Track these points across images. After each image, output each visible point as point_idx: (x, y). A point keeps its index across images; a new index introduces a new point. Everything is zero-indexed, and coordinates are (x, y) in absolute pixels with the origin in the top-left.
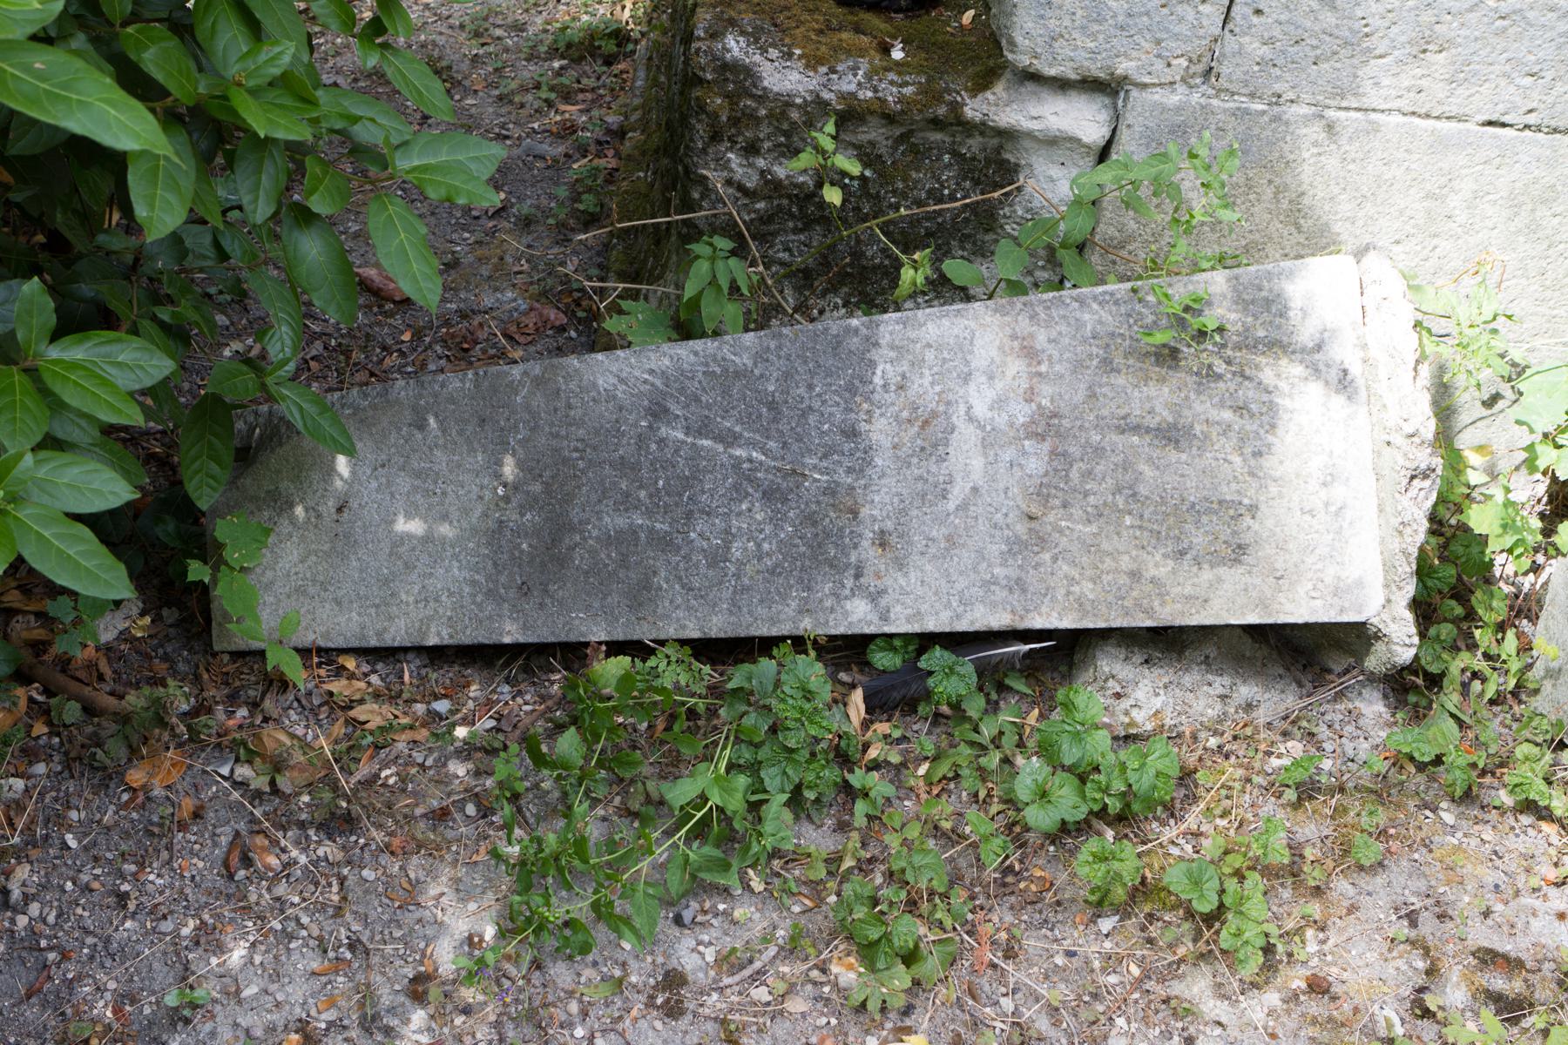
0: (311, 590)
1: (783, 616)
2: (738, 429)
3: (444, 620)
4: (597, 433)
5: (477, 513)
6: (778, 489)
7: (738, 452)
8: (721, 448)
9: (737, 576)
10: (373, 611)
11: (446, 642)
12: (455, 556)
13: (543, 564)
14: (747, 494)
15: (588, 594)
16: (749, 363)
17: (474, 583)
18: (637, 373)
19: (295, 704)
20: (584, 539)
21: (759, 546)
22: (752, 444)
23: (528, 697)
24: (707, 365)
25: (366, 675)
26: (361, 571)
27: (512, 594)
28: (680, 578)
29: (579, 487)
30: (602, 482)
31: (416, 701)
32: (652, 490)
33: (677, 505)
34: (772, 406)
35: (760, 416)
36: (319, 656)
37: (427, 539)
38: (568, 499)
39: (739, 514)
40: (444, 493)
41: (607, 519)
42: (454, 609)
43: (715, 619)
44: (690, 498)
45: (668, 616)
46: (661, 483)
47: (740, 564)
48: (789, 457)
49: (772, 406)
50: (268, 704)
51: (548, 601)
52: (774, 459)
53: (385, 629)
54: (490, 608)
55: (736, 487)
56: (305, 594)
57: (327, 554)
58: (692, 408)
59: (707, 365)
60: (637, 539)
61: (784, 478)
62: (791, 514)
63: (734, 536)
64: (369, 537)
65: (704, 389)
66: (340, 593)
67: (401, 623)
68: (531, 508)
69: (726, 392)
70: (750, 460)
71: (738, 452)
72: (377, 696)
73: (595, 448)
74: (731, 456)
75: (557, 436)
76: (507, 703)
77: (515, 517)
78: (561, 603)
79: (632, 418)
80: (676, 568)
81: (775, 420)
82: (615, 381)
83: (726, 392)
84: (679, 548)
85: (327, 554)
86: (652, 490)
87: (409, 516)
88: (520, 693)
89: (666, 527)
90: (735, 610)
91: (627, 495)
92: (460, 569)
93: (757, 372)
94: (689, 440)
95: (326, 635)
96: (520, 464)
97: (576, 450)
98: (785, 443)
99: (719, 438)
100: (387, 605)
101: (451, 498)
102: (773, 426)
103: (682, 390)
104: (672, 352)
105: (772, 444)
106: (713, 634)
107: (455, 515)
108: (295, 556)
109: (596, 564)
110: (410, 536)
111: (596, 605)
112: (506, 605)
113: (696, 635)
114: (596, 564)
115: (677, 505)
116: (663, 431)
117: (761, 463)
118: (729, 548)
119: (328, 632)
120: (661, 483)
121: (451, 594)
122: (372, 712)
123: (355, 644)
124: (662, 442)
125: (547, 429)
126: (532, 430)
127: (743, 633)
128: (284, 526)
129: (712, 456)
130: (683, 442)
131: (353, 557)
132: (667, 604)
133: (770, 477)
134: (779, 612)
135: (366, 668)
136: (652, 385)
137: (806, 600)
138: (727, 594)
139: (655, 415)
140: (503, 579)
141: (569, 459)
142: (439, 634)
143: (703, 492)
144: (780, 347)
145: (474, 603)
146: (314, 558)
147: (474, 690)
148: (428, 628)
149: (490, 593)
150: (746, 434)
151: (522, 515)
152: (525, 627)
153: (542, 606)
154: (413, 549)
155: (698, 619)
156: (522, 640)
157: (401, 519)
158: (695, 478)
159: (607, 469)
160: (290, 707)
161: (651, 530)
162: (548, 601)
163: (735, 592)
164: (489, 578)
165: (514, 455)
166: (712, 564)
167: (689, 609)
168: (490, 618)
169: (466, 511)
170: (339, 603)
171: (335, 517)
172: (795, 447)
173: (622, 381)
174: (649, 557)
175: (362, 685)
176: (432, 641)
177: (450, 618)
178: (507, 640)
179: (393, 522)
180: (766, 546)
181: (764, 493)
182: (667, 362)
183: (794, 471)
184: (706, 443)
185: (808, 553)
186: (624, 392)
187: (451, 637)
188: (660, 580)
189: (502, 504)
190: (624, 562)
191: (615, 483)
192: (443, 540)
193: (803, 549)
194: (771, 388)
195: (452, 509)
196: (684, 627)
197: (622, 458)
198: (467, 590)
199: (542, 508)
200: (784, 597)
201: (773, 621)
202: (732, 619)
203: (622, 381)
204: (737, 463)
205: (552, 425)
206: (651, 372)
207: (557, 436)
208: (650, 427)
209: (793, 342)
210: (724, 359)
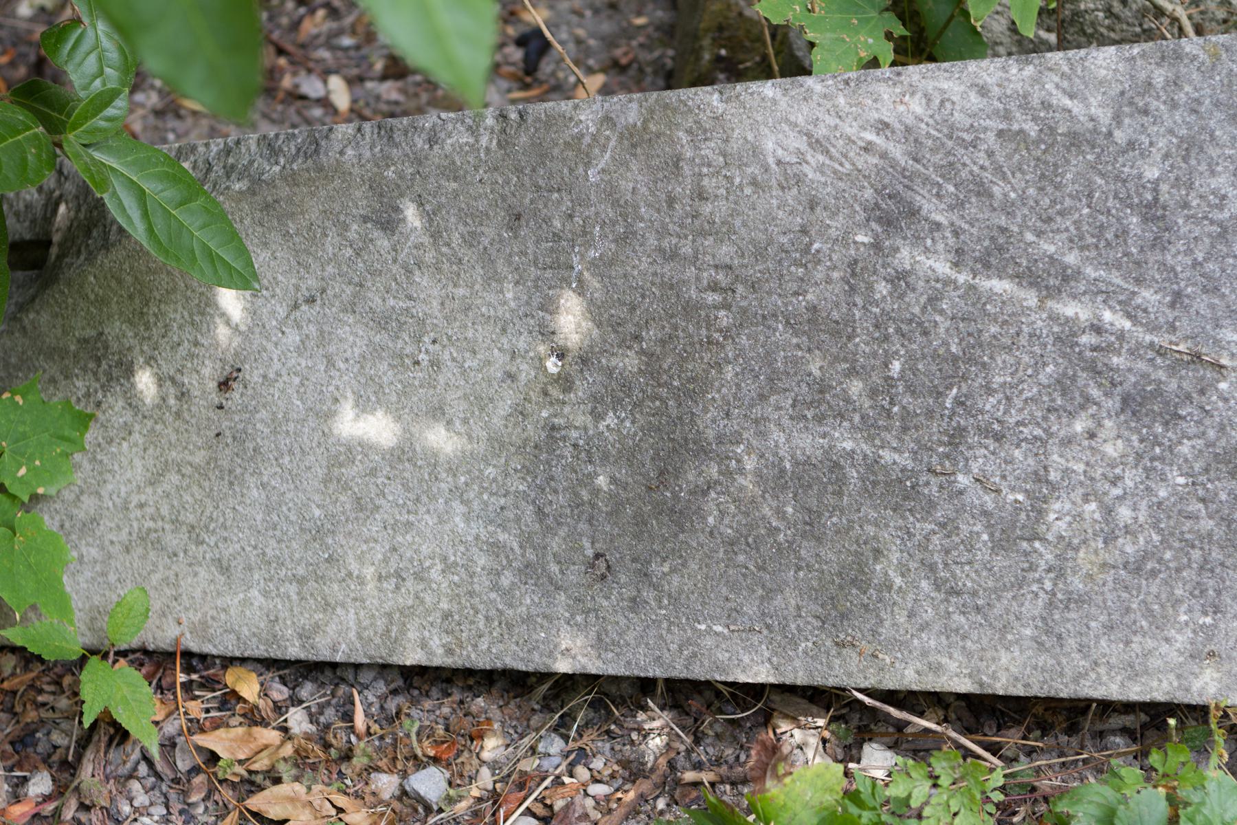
0: (172, 541)
1: (1153, 663)
2: (1071, 259)
3: (436, 617)
4: (760, 254)
5: (504, 408)
6: (1158, 392)
7: (1070, 309)
8: (1031, 298)
9: (1058, 572)
10: (292, 589)
11: (437, 662)
12: (458, 493)
13: (640, 521)
14: (1088, 400)
15: (734, 586)
16: (1104, 117)
17: (495, 548)
18: (850, 129)
19: (143, 769)
20: (728, 473)
21: (1108, 511)
22: (1107, 295)
23: (598, 764)
24: (1007, 116)
25: (278, 708)
26: (268, 509)
27: (575, 574)
28: (932, 568)
29: (719, 366)
30: (768, 358)
31: (377, 769)
32: (876, 379)
33: (930, 414)
34: (1153, 212)
35: (1123, 234)
36: (188, 669)
37: (402, 454)
38: (695, 389)
39: (1068, 442)
40: (435, 364)
41: (777, 436)
42: (455, 598)
43: (1004, 658)
44: (959, 402)
45: (903, 645)
46: (896, 366)
47: (1066, 546)
48: (1184, 326)
49: (1153, 212)
50: (87, 772)
51: (649, 595)
52: (1153, 328)
53: (317, 627)
54: (528, 600)
55: (1063, 384)
56: (158, 545)
57: (201, 472)
58: (972, 210)
59: (1007, 116)
60: (842, 481)
61: (1172, 370)
62: (1185, 449)
63: (1054, 487)
64: (284, 442)
65: (998, 170)
66: (228, 551)
67: (349, 617)
68: (617, 403)
69: (1048, 178)
70: (1097, 329)
71: (1070, 309)
72: (301, 761)
73: (753, 287)
74: (1054, 318)
75: (673, 256)
76: (558, 782)
77: (580, 420)
78: (675, 600)
79: (836, 225)
80: (923, 547)
81: (1158, 244)
82: (802, 144)
83: (1048, 178)
84: (932, 505)
85: (201, 472)
86: (876, 379)
87: (364, 406)
88: (582, 756)
89: (905, 460)
90: (1049, 641)
91: (823, 388)
92: (467, 518)
93: (1120, 136)
94: (962, 278)
95: (201, 629)
96: (595, 311)
97: (714, 287)
98: (1178, 295)
99: (1028, 278)
100: (320, 579)
101: (448, 374)
102: (1153, 257)
103: (949, 169)
104: (930, 85)
105: (1147, 296)
106: (1001, 687)
107: (457, 408)
108: (139, 471)
109: (751, 527)
110: (365, 447)
111: (751, 609)
112: (562, 597)
113: (964, 686)
114: (751, 527)
115: (930, 414)
116: (905, 256)
117: (1121, 336)
118: (1041, 513)
119: (204, 623)
120: (896, 366)
121: (448, 568)
122: (292, 800)
123: (261, 651)
124: (901, 279)
125: (652, 241)
126: (624, 239)
127: (1065, 691)
128: (115, 411)
129: (1012, 316)
130: (948, 282)
131: (252, 481)
132: (902, 620)
133: (1141, 366)
134: (1147, 654)
135: (280, 692)
136: (884, 155)
137: (1209, 632)
138: (1033, 607)
139: (888, 222)
140: (555, 544)
141: (699, 306)
142: (424, 645)
143: (989, 391)
144: (1176, 83)
145: (495, 587)
146: (175, 478)
147: (492, 747)
148: (403, 631)
149: (527, 571)
150: (1090, 271)
151: (598, 417)
152: (600, 644)
153: (635, 603)
154: (373, 472)
155: (969, 655)
156: (594, 667)
157: (347, 411)
158: (971, 360)
159: (781, 333)
160: (131, 776)
161: (873, 464)
162: (649, 595)
163: (1051, 605)
164: (526, 541)
165: (581, 290)
166: (1003, 543)
167: (948, 631)
168: (528, 620)
169: (481, 403)
170: (225, 569)
171: (215, 398)
172: (1201, 304)
173: (817, 144)
174: (864, 521)
175: (270, 736)
176: (413, 657)
177: (447, 615)
178: (563, 666)
179: (330, 415)
180: (1124, 513)
181: (1126, 400)
182: (916, 106)
183: (1197, 357)
184: (1000, 286)
185: (1219, 533)
186: (821, 169)
187: (449, 652)
188: (888, 568)
189: (555, 392)
190: (811, 527)
191: (795, 362)
192: (433, 459)
193: (1207, 524)
194: (1152, 173)
195: (451, 396)
196: (937, 669)
197: (813, 309)
198: (482, 561)
199: (637, 405)
200: (1159, 623)
201: (1133, 672)
202: (1043, 659)
203: (817, 144)
204: (1067, 336)
205: (663, 232)
206: (883, 127)
207: (673, 256)
208: (877, 246)
209: (1207, 72)
210: (1046, 105)
